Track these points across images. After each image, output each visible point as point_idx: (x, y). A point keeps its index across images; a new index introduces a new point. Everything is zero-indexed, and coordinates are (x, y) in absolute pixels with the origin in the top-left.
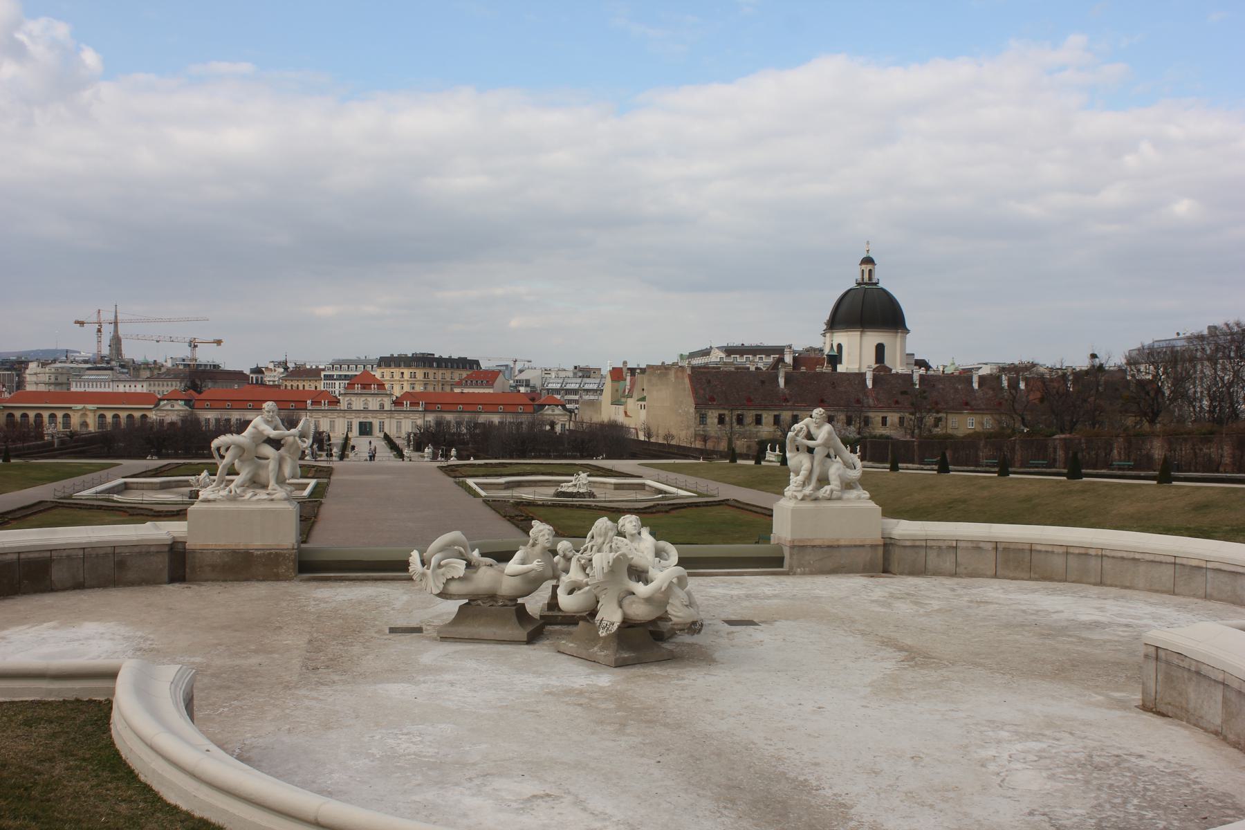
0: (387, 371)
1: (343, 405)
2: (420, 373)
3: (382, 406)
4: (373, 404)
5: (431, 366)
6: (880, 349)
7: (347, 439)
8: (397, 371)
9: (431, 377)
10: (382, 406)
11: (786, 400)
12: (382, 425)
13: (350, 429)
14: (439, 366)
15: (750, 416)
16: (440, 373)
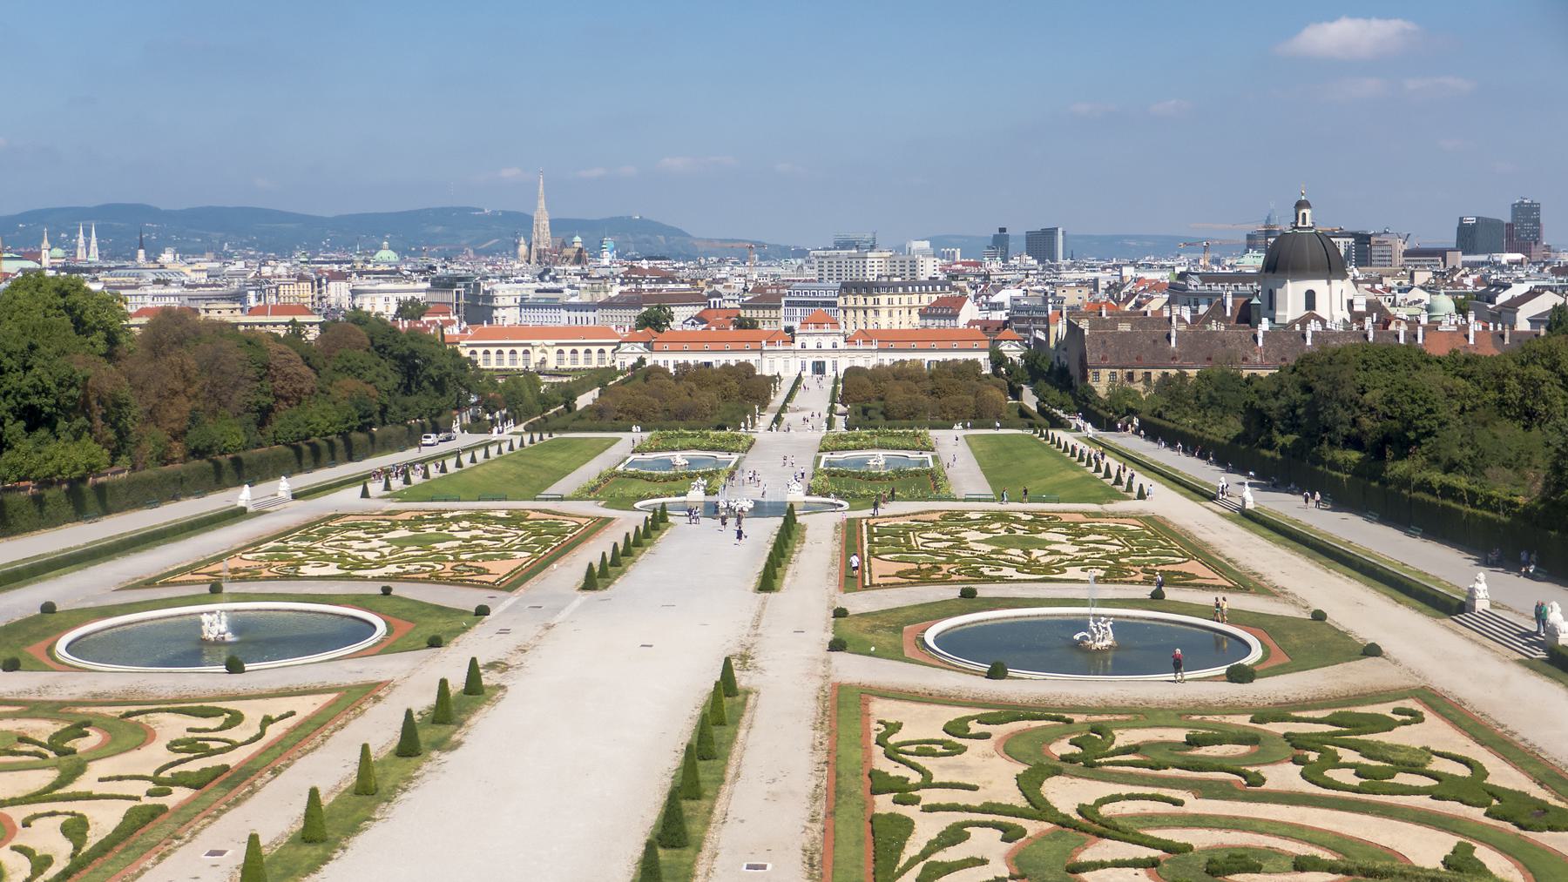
0: (851, 299)
1: (797, 345)
2: (884, 299)
3: (835, 345)
4: (827, 343)
5: (896, 292)
6: (1310, 297)
7: (799, 379)
8: (861, 299)
9: (896, 302)
10: (835, 345)
11: (1174, 358)
12: (835, 364)
13: (804, 368)
14: (905, 291)
15: (1139, 374)
16: (905, 298)
